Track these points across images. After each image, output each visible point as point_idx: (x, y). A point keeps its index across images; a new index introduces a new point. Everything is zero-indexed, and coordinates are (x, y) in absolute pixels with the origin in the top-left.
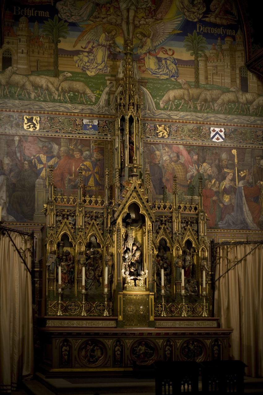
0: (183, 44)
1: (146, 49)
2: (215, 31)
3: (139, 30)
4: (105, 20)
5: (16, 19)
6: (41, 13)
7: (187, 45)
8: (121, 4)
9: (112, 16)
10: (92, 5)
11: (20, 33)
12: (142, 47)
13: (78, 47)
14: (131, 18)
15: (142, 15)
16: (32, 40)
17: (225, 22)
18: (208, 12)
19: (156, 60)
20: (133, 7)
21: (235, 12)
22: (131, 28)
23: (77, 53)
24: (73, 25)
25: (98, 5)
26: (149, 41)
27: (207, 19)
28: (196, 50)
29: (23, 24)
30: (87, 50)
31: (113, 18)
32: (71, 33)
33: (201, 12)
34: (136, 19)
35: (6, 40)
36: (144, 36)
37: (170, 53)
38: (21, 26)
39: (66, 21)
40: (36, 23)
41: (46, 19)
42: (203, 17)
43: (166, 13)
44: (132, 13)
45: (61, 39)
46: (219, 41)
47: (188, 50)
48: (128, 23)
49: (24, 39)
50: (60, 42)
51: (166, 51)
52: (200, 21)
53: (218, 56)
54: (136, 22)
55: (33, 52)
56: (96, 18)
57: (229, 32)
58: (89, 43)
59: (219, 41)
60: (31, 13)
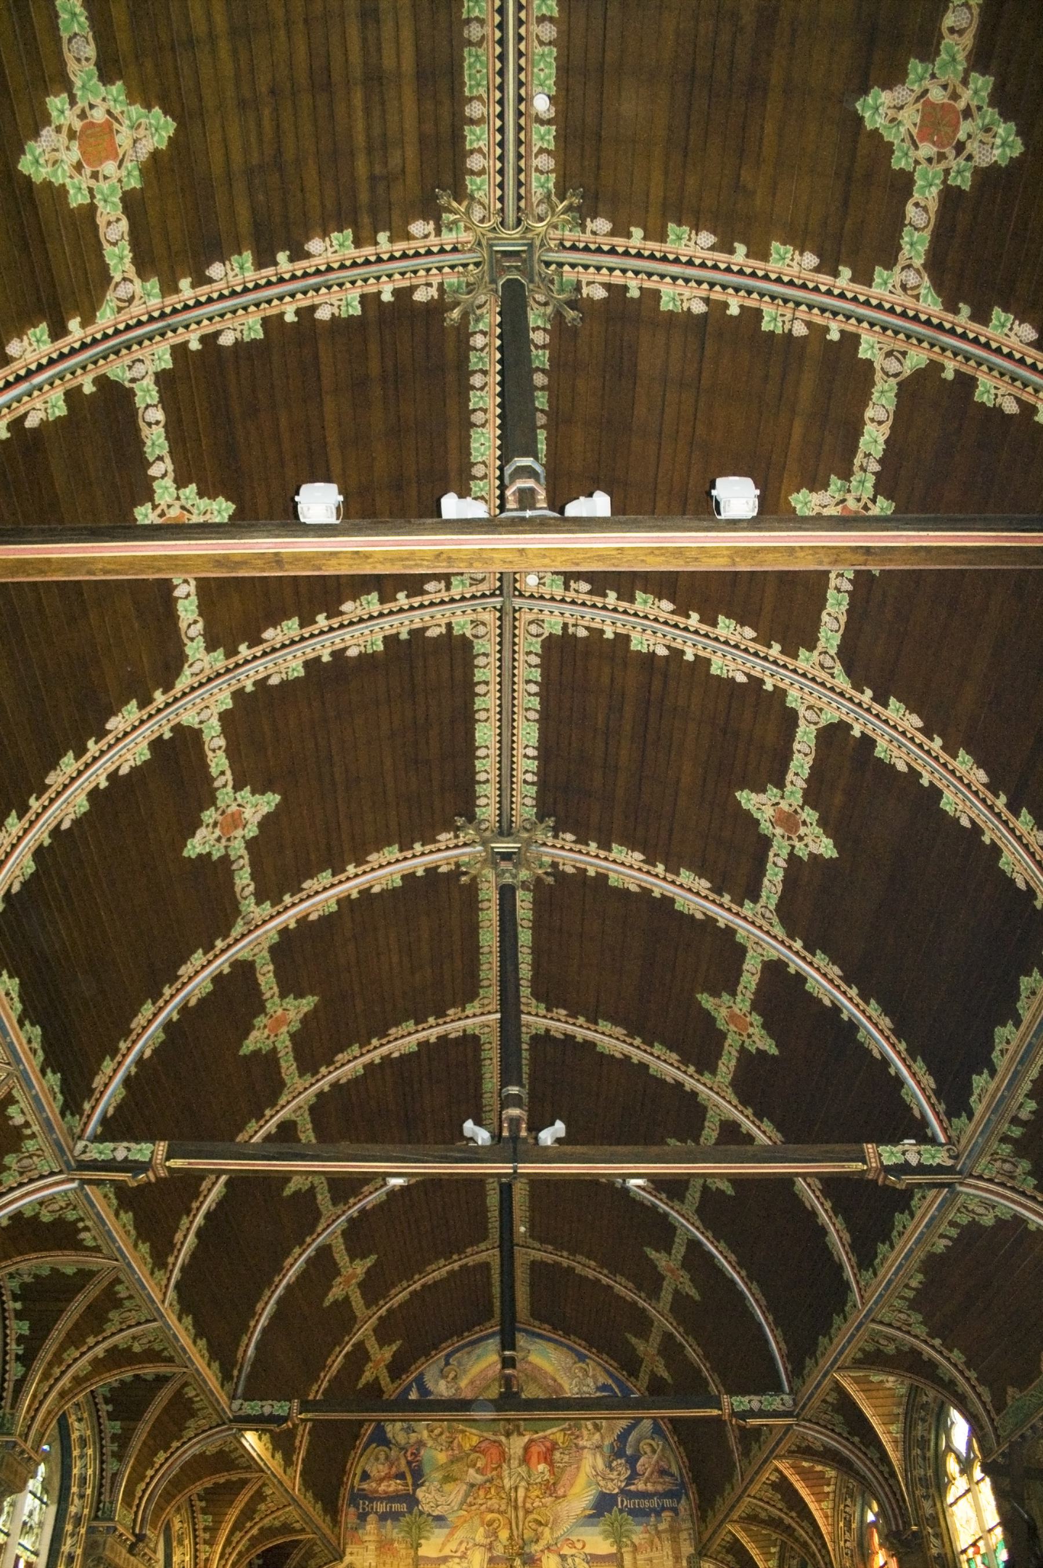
0: (597, 1529)
1: (542, 1544)
2: (646, 1504)
3: (531, 1517)
4: (483, 1507)
5: (363, 1517)
6: (396, 1507)
7: (605, 1531)
8: (506, 1481)
9: (494, 1501)
10: (465, 1487)
11: (366, 1538)
12: (537, 1541)
13: (446, 1552)
14: (520, 1500)
15: (537, 1493)
16: (384, 1546)
17: (660, 1488)
18: (634, 1476)
19: (558, 1559)
20: (523, 1484)
21: (674, 1470)
22: (521, 1514)
23: (445, 1559)
24: (440, 1519)
25: (472, 1485)
26: (547, 1531)
27: (632, 1488)
28: (618, 1536)
29: (371, 1526)
30: (459, 1554)
31: (494, 1503)
32: (437, 1531)
33: (622, 1478)
34: (529, 1500)
35: (348, 1550)
36: (540, 1524)
37: (579, 1545)
38: (368, 1527)
39: (429, 1515)
40: (389, 1522)
41: (403, 1514)
42: (627, 1485)
43: (572, 1485)
44: (521, 1493)
45: (422, 1541)
46: (653, 1519)
47: (607, 1538)
48: (516, 1508)
49: (372, 1547)
50: (419, 1545)
51: (573, 1543)
52: (622, 1491)
53: (652, 1542)
54: (528, 1505)
55: (384, 1564)
56: (471, 1505)
57: (667, 1502)
58: (461, 1543)
59: (653, 1519)
60: (381, 1507)
